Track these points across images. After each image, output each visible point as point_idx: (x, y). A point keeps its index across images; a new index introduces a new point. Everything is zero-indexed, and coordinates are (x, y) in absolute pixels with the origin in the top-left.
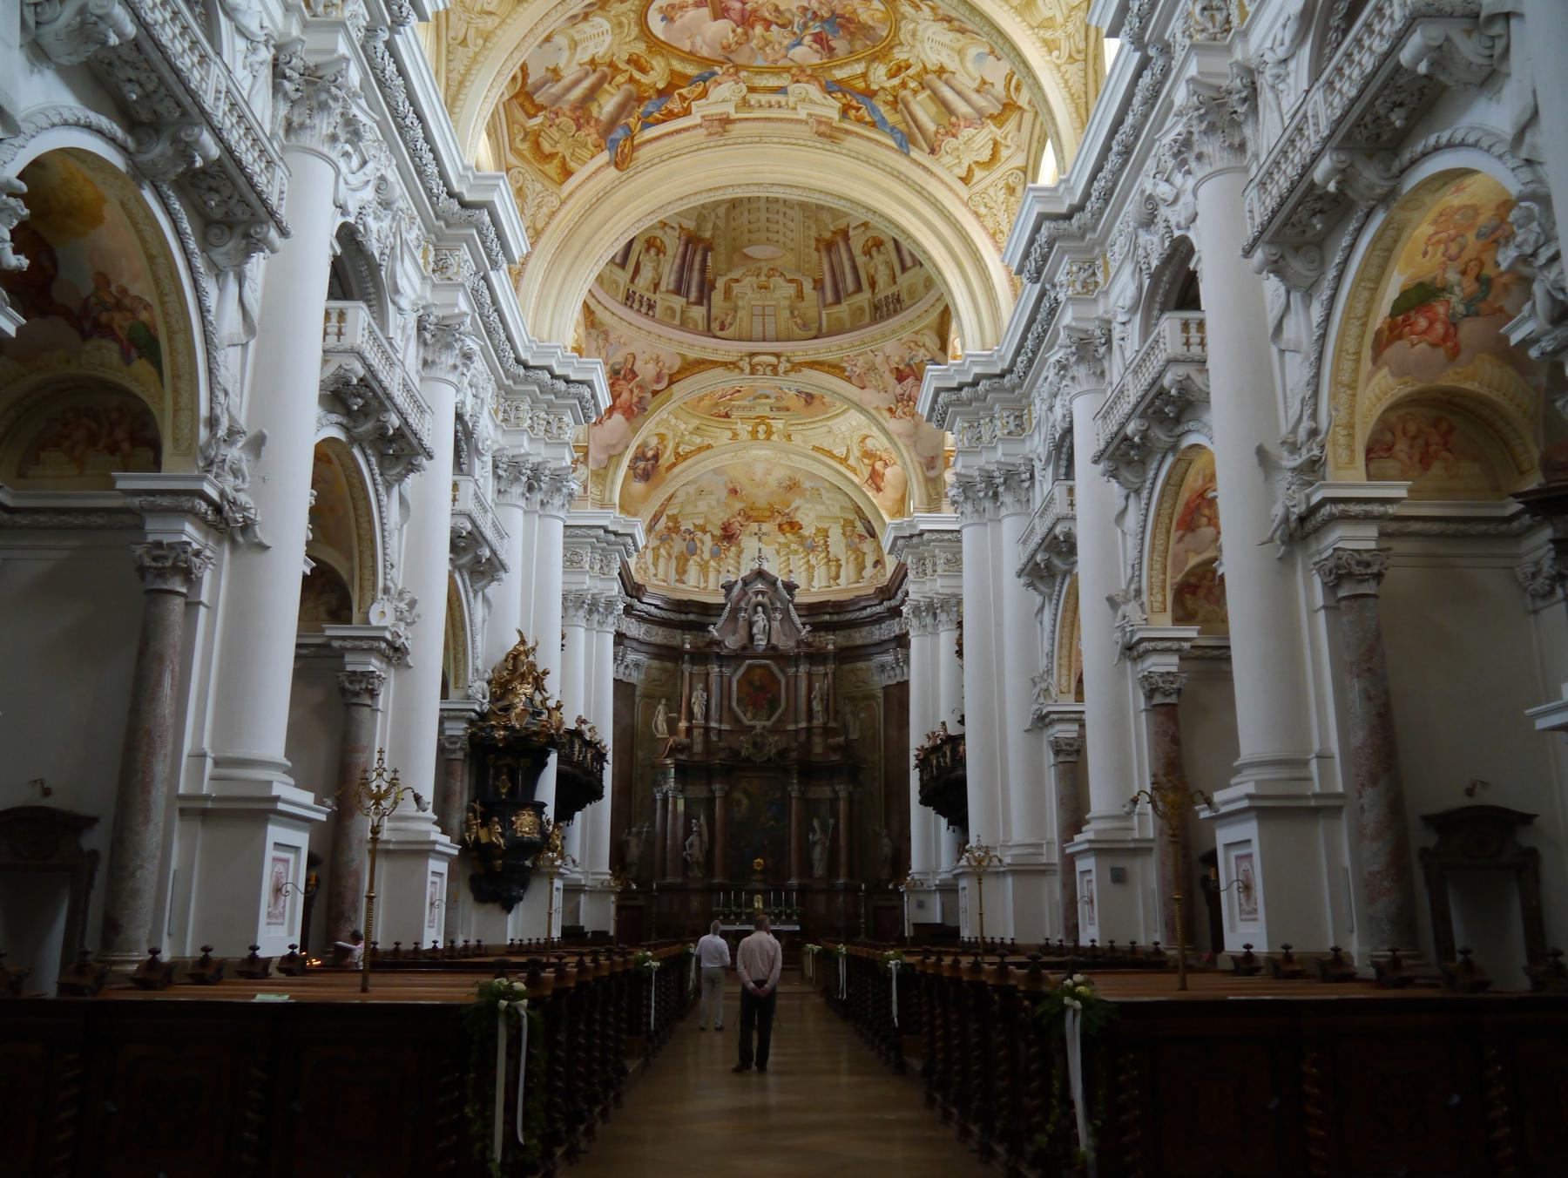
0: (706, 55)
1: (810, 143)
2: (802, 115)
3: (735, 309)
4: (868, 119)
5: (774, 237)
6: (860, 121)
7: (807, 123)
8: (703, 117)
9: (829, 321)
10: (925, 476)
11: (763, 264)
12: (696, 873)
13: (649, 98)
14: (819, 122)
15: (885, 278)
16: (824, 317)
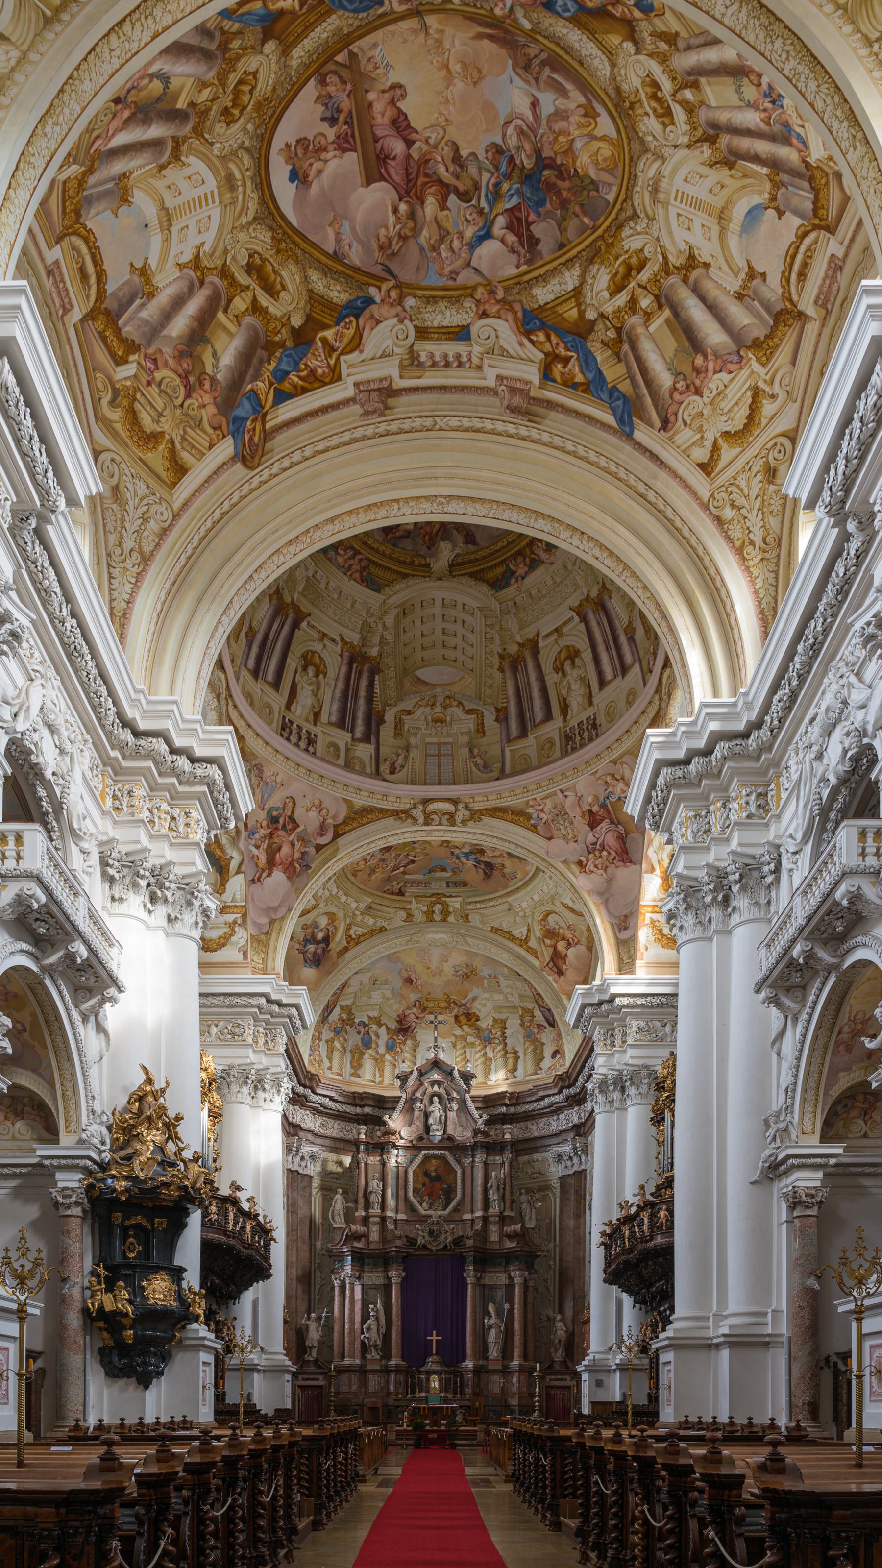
0: (357, 262)
1: (500, 426)
2: (491, 382)
3: (408, 748)
4: (579, 378)
5: (450, 654)
6: (570, 384)
7: (496, 393)
8: (356, 385)
9: (513, 756)
10: (616, 938)
11: (438, 690)
12: (374, 1355)
13: (283, 345)
14: (513, 390)
15: (580, 699)
16: (507, 750)
